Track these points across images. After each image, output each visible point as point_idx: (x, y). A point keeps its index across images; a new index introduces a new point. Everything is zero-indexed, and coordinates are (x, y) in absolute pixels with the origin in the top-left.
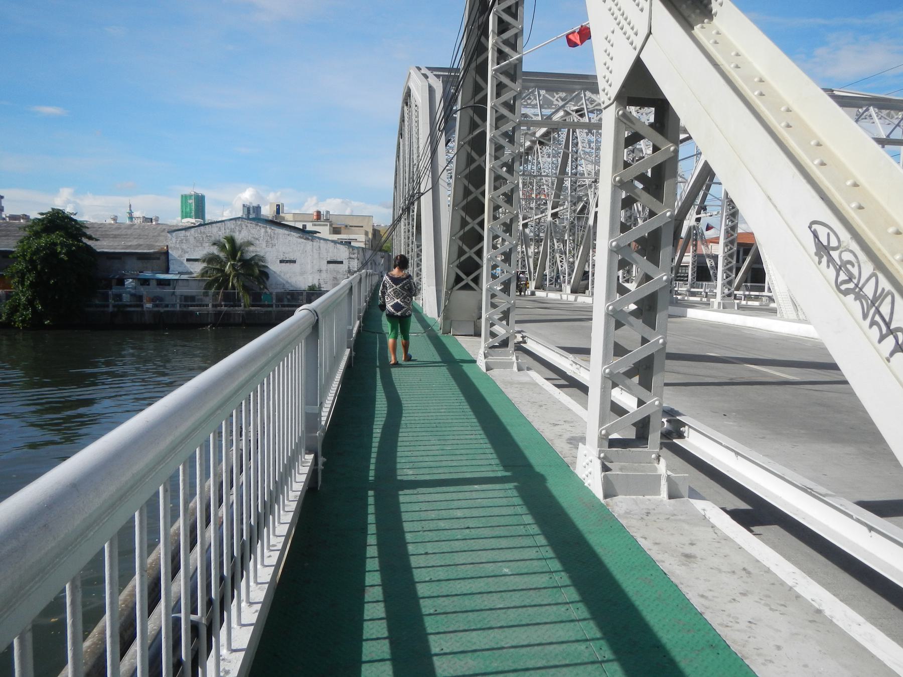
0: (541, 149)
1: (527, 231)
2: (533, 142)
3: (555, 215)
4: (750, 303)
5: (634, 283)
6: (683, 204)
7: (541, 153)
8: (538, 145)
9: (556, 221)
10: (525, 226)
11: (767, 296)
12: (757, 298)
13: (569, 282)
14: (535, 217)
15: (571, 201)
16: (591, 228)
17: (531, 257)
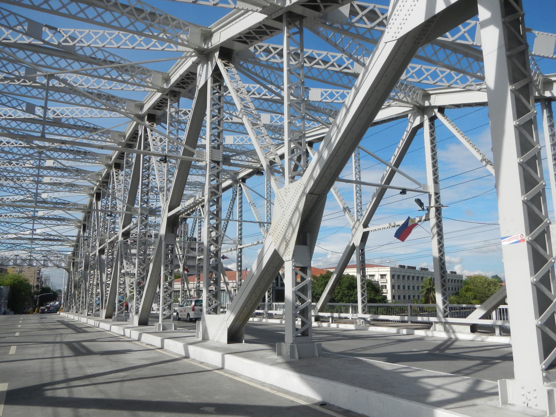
0: (116, 172)
1: (104, 257)
2: (109, 167)
3: (126, 235)
4: (342, 326)
5: (228, 313)
6: (333, 156)
7: (117, 176)
8: (114, 169)
9: (127, 241)
10: (102, 252)
11: (361, 318)
12: (345, 320)
13: (137, 313)
14: (109, 241)
15: (141, 214)
16: (163, 239)
17: (104, 283)
